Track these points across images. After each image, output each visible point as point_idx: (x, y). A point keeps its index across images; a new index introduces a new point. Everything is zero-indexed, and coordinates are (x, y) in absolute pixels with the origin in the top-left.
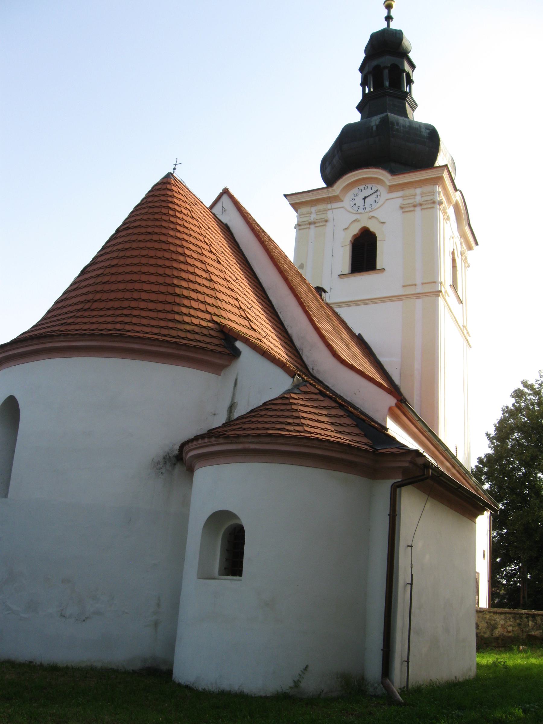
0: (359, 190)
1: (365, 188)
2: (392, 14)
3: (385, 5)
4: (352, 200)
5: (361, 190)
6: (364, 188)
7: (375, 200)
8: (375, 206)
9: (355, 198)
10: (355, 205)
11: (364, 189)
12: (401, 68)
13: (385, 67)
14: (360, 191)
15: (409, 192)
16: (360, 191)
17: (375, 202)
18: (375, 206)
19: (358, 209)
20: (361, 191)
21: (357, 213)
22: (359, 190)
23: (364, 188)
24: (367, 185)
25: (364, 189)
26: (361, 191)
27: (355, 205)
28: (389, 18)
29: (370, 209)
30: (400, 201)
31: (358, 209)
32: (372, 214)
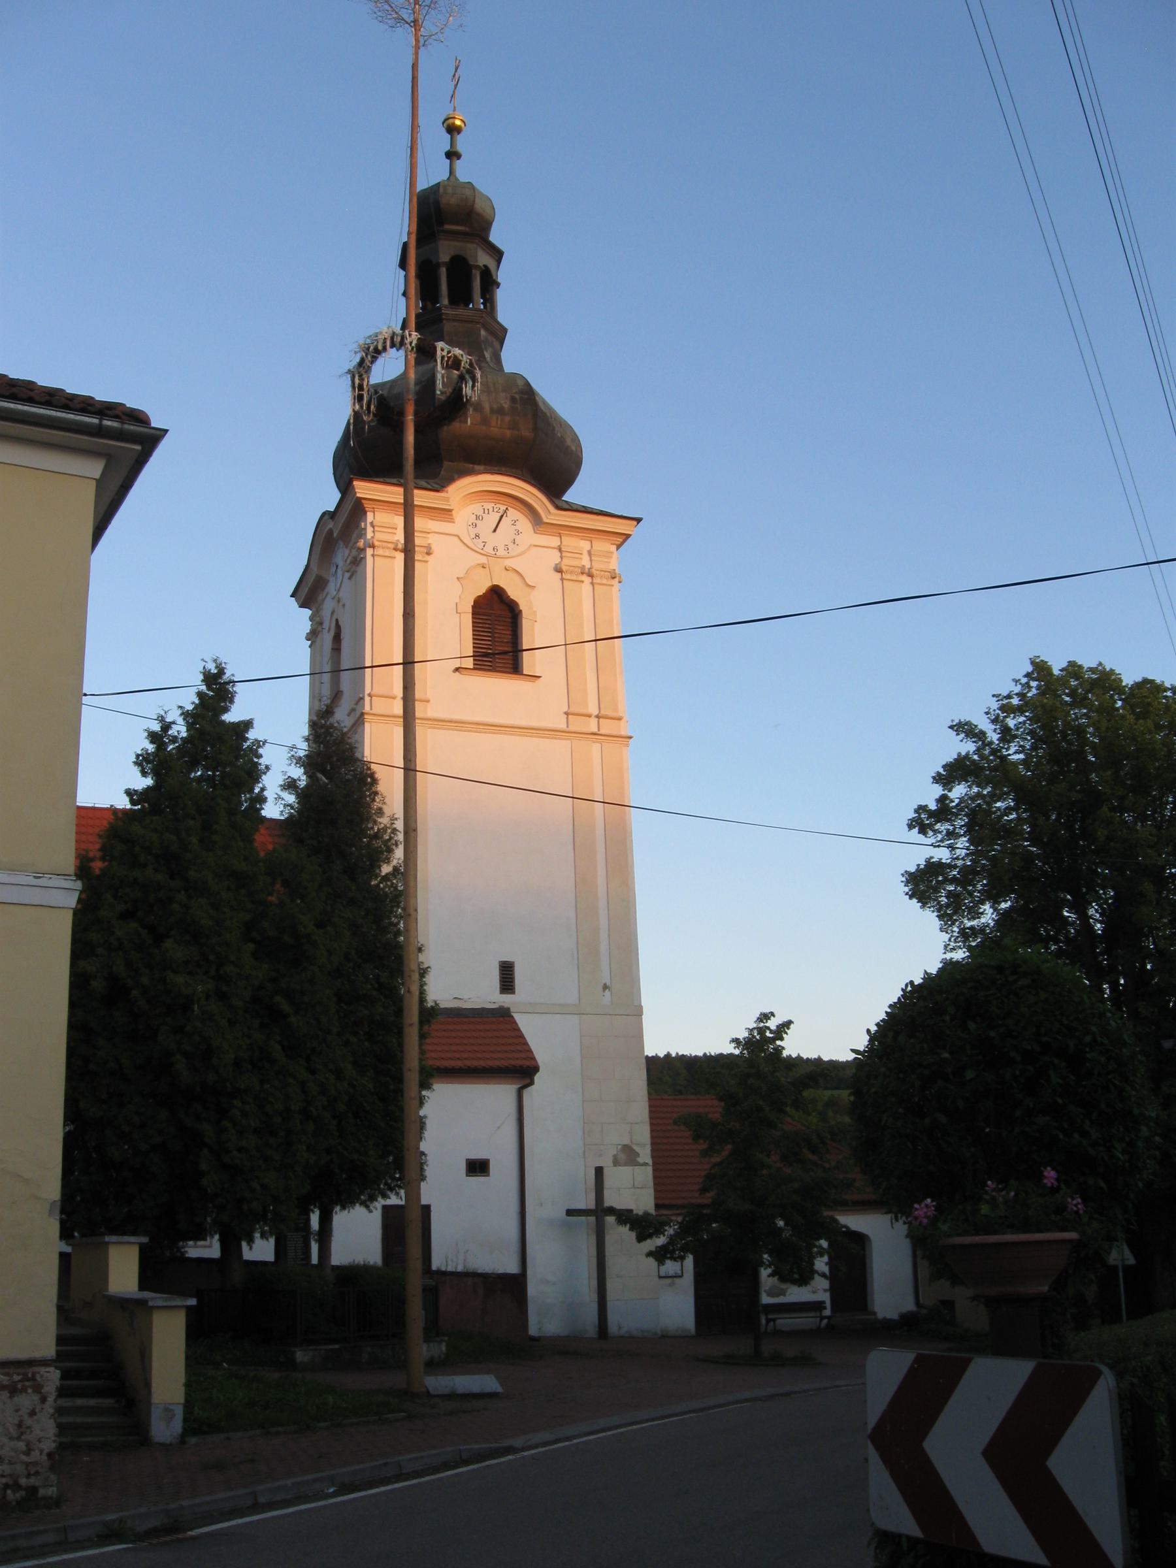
0: (484, 509)
1: (496, 510)
2: (460, 148)
3: (445, 125)
4: (471, 526)
5: (488, 510)
6: (493, 507)
7: (514, 540)
8: (514, 550)
9: (477, 522)
10: (477, 536)
11: (493, 511)
12: (494, 277)
13: (477, 267)
14: (486, 512)
15: (570, 542)
16: (486, 512)
17: (514, 543)
18: (514, 550)
19: (484, 546)
20: (488, 513)
21: (478, 550)
22: (484, 509)
23: (493, 507)
24: (498, 505)
25: (493, 511)
26: (488, 513)
27: (477, 536)
28: (452, 155)
29: (506, 552)
30: (555, 557)
31: (484, 546)
32: (508, 563)
